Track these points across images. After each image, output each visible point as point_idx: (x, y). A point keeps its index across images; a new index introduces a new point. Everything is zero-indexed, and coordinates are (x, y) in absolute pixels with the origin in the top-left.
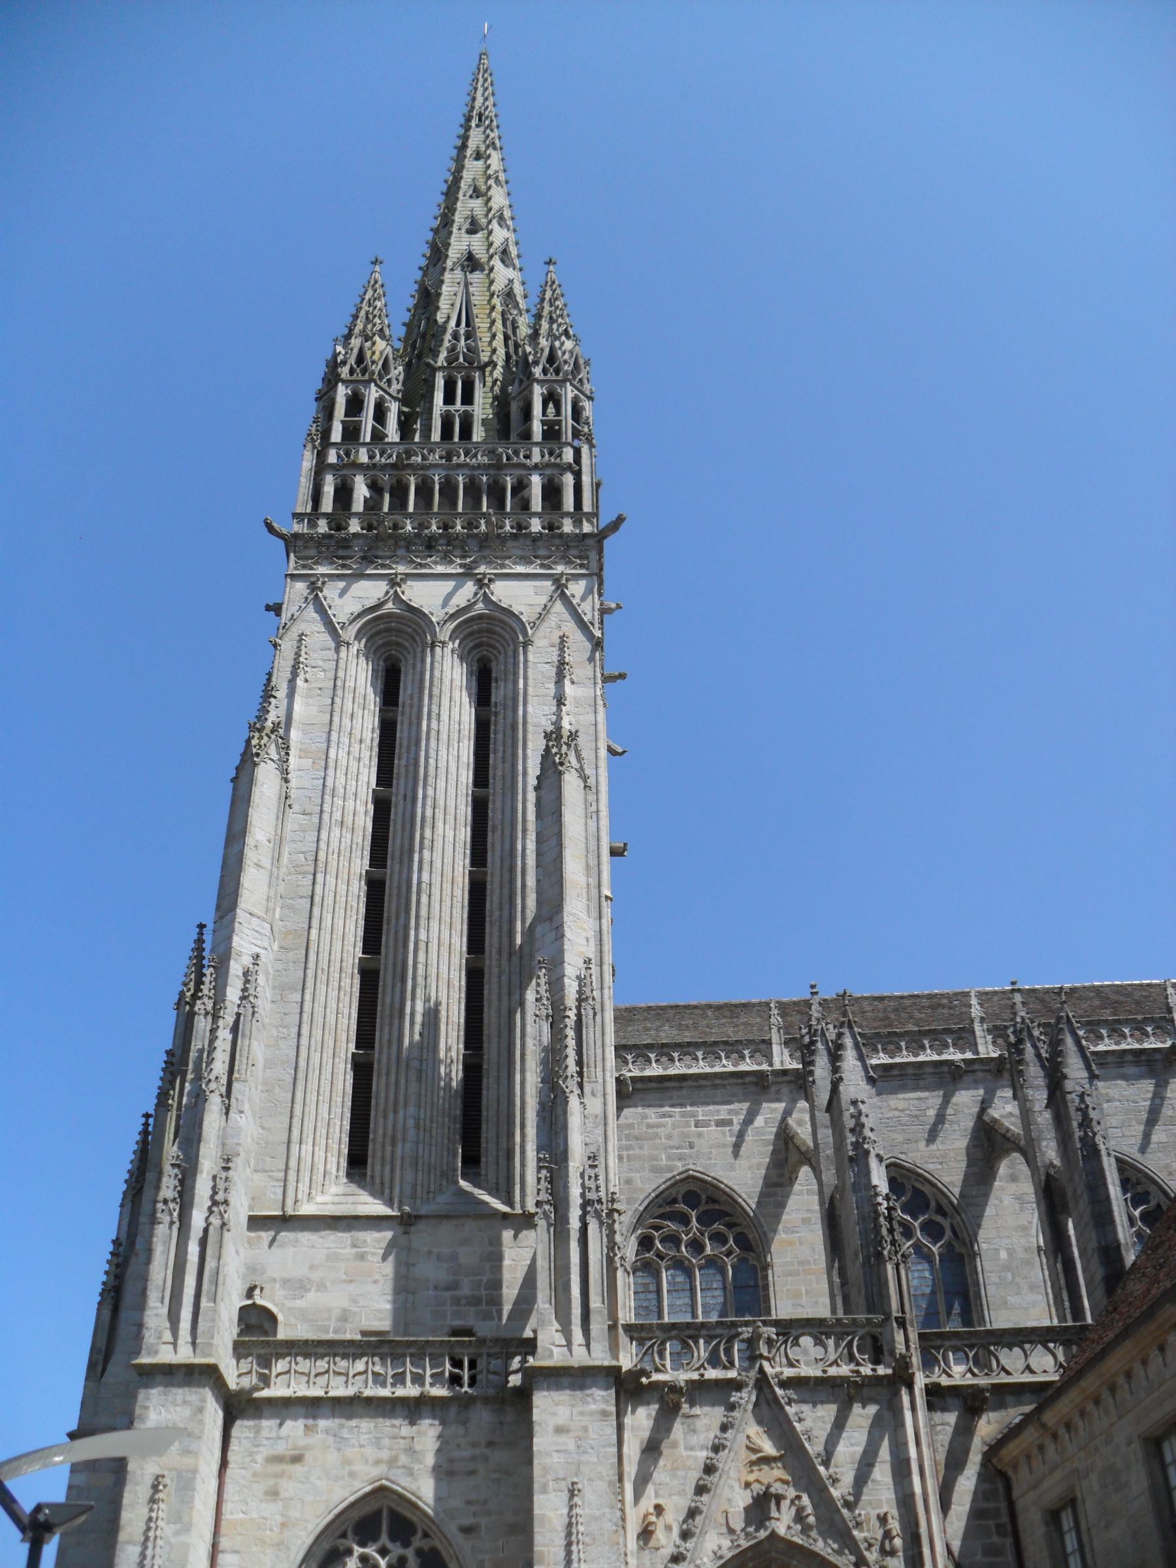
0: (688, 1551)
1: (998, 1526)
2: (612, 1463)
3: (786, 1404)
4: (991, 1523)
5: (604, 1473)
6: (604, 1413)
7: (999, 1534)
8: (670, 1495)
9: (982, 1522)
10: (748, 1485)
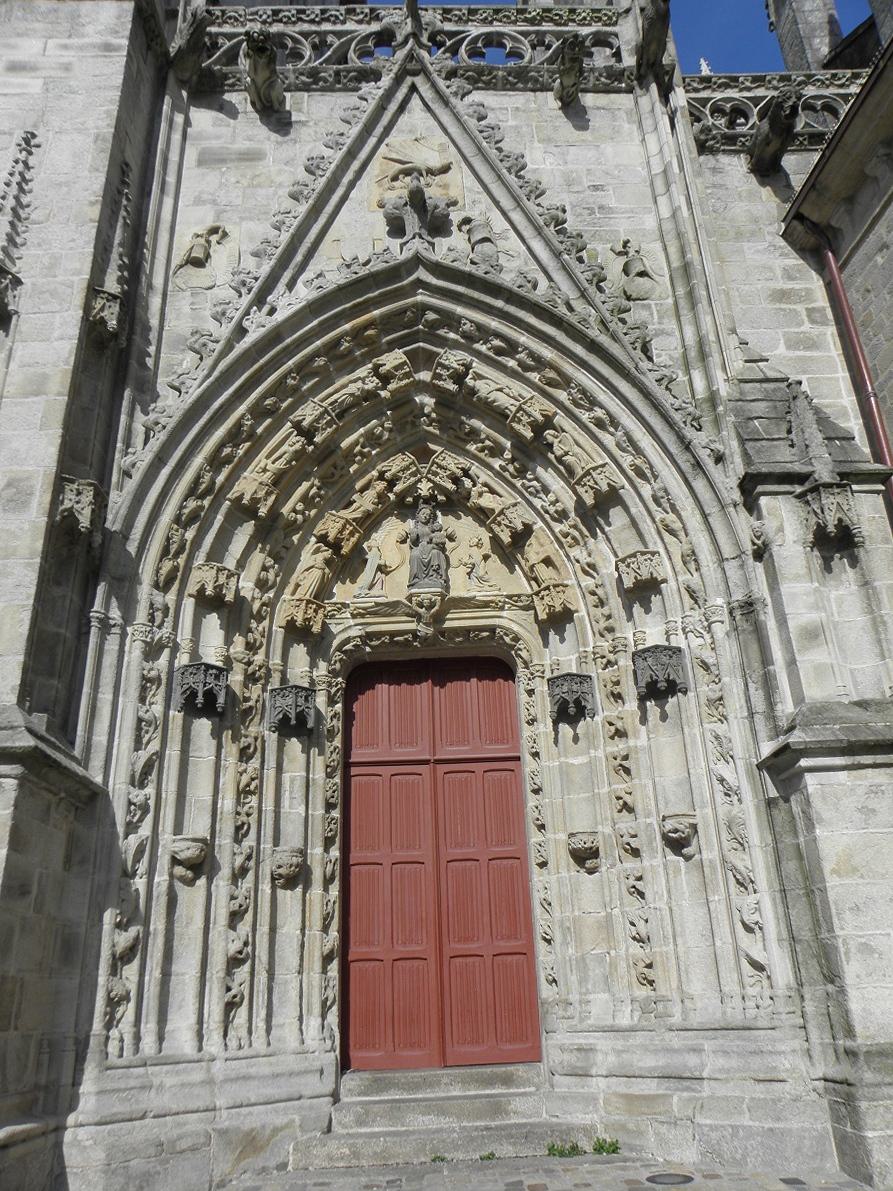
0: (256, 279)
1: (810, 312)
2: (108, 112)
3: (456, 94)
4: (800, 308)
5: (90, 124)
6: (108, 47)
7: (813, 321)
8: (242, 219)
9: (783, 306)
10: (381, 206)
